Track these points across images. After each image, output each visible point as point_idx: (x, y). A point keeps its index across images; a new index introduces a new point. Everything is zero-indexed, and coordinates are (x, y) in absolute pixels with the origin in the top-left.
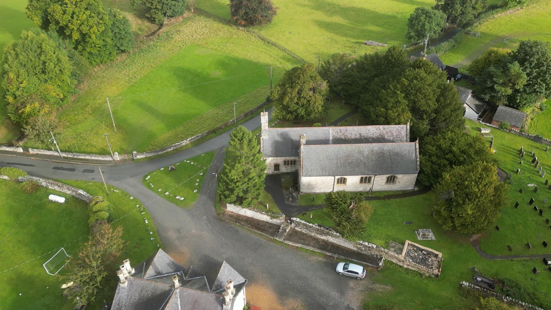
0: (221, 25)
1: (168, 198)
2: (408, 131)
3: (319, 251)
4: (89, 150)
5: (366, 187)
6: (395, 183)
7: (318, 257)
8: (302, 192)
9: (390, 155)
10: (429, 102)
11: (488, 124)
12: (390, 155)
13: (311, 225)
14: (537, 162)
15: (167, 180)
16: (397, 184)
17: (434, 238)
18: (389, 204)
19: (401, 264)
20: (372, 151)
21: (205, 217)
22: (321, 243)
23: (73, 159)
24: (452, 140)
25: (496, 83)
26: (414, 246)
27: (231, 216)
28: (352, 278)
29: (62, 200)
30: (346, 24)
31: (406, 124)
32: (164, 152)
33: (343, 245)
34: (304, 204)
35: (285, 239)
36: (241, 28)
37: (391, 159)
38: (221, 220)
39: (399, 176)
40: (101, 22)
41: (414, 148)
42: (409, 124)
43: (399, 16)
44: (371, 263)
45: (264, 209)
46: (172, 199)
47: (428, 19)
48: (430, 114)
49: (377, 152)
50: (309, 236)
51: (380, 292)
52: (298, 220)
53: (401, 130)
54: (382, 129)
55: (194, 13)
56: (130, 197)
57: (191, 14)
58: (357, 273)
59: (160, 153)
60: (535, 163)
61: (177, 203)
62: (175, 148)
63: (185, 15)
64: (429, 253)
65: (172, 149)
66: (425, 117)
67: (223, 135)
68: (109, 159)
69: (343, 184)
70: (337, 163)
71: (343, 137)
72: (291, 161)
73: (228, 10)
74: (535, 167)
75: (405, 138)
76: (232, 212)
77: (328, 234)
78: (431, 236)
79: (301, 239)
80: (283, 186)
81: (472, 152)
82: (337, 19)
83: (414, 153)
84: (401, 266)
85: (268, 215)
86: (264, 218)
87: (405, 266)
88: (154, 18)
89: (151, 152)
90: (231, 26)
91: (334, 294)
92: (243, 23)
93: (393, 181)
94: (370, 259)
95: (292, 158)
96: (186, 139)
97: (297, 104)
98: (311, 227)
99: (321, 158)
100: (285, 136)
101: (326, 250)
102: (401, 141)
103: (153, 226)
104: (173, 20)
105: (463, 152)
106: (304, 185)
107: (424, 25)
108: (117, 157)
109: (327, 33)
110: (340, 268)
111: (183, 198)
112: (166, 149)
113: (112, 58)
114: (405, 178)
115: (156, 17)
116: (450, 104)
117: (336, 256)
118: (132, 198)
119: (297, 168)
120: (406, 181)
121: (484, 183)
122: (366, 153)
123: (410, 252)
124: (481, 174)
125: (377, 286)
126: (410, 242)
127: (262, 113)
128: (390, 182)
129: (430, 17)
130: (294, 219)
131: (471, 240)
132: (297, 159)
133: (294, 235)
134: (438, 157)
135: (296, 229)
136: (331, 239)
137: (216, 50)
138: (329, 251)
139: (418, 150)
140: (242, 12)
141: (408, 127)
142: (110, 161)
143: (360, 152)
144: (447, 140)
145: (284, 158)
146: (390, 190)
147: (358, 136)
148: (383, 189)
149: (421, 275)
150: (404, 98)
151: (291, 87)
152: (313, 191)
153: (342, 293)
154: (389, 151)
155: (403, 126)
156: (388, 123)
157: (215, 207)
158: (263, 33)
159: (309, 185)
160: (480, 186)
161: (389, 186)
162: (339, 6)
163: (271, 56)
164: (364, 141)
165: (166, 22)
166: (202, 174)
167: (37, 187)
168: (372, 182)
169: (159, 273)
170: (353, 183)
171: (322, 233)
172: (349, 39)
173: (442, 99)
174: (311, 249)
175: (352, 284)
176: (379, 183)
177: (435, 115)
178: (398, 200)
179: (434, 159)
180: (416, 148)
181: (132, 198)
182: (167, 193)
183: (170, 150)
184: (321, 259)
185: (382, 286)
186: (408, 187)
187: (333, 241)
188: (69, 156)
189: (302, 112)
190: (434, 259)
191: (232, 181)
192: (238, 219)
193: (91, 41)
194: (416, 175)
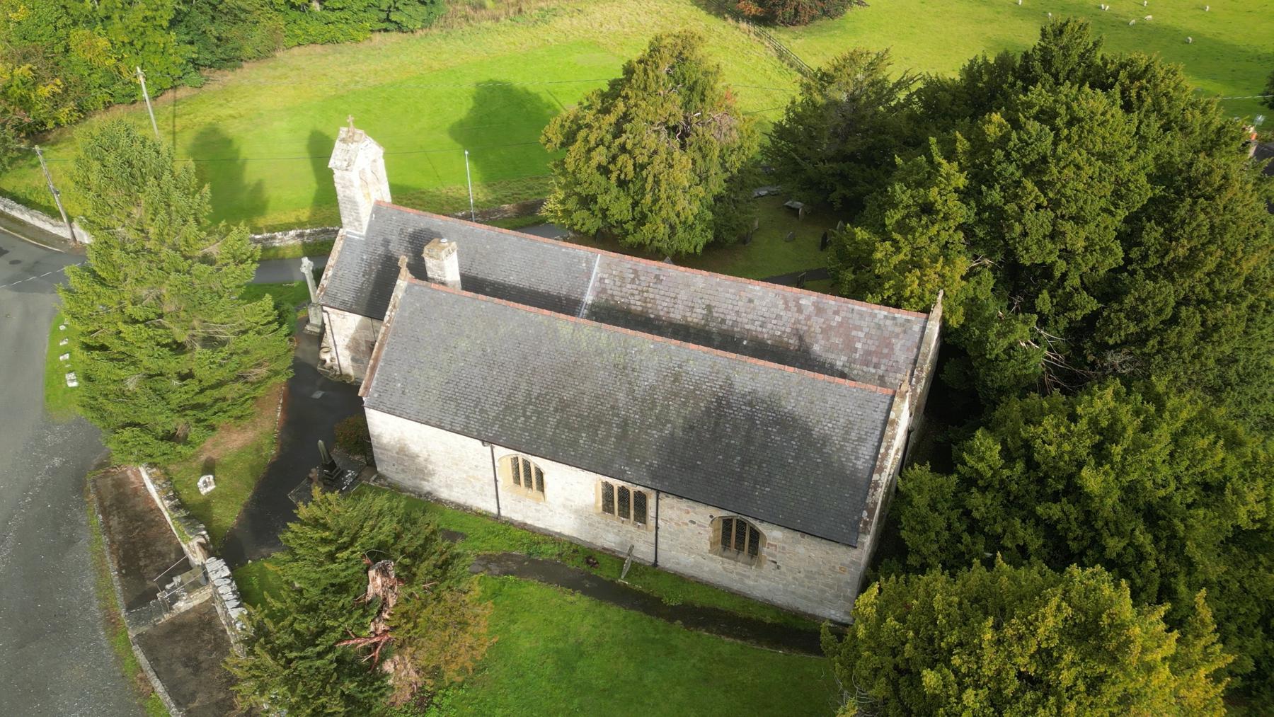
5: (612, 534)
6: (759, 566)
8: (380, 477)
9: (750, 418)
10: (1068, 226)
12: (750, 418)
16: (767, 567)
20: (677, 378)
24: (1107, 435)
27: (120, 484)
37: (749, 440)
39: (773, 535)
41: (879, 417)
42: (937, 312)
48: (1070, 295)
49: (697, 386)
66: (1044, 302)
69: (534, 491)
70: (516, 388)
71: (637, 305)
81: (1201, 528)
83: (873, 440)
90: (725, 19)
93: (754, 551)
99: (464, 345)
105: (1153, 516)
106: (384, 448)
116: (1188, 264)
122: (649, 378)
124: (1047, 657)
128: (740, 547)
134: (1012, 503)
141: (934, 328)
142: (66, 240)
144: (1083, 424)
146: (736, 586)
147: (696, 317)
148: (705, 575)
152: (427, 487)
156: (858, 292)
159: (403, 455)
161: (729, 564)
164: (718, 340)
168: (651, 523)
170: (567, 501)
173: (1153, 234)
176: (682, 535)
178: (727, 645)
179: (979, 503)
189: (620, 208)
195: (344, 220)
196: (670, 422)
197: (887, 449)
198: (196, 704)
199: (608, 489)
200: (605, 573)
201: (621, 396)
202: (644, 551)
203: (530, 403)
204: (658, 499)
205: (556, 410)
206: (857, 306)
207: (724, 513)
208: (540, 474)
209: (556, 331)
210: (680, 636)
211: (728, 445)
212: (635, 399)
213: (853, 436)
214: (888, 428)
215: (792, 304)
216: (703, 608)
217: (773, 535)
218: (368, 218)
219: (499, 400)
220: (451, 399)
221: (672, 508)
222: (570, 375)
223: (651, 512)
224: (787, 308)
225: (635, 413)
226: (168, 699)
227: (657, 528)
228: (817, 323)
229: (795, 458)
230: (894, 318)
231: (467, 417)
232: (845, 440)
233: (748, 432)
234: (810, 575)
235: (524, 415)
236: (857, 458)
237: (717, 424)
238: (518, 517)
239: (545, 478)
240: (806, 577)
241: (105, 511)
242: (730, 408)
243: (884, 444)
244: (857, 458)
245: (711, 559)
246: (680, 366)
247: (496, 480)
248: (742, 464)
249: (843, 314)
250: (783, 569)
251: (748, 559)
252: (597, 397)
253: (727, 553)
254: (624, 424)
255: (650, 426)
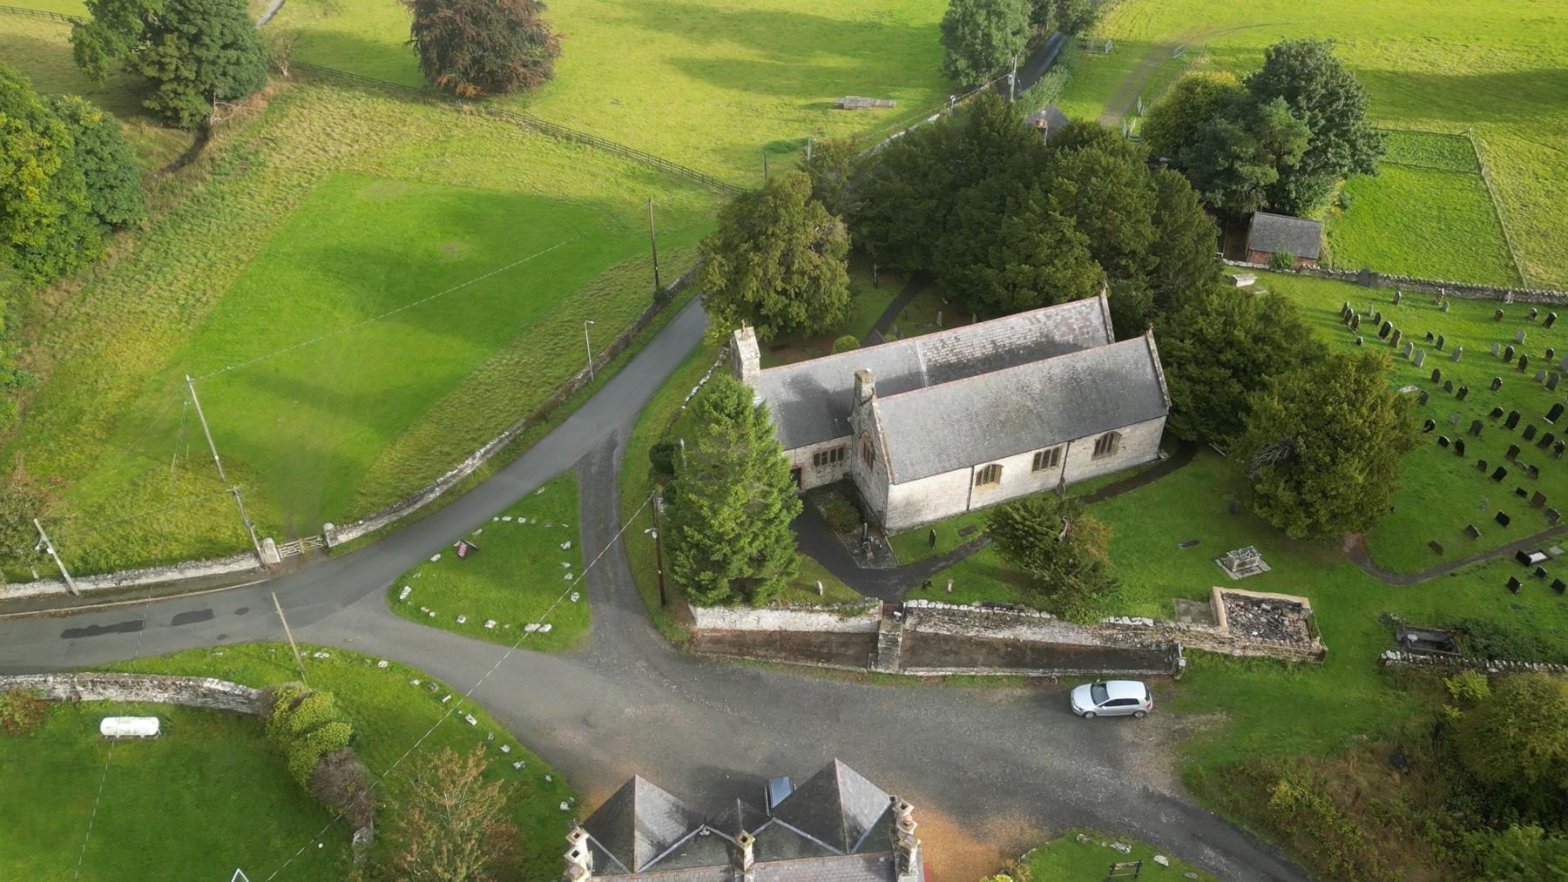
0: (398, 107)
1: (500, 636)
2: (1107, 313)
3: (1007, 672)
4: (156, 552)
5: (1051, 477)
7: (1009, 690)
11: (1244, 264)
13: (964, 608)
14: (1397, 333)
15: (469, 584)
16: (1120, 451)
17: (1266, 567)
19: (1226, 650)
20: (1050, 379)
21: (641, 664)
22: (1003, 650)
23: (119, 591)
25: (1238, 157)
26: (1237, 597)
28: (1120, 718)
29: (148, 726)
30: (756, 59)
31: (1098, 294)
32: (418, 505)
33: (1061, 640)
34: (912, 559)
35: (903, 666)
36: (466, 107)
37: (1099, 392)
38: (693, 660)
41: (1145, 351)
42: (1104, 294)
43: (886, 22)
44: (1150, 667)
45: (812, 598)
46: (511, 635)
47: (994, 19)
50: (962, 641)
51: (1206, 733)
52: (924, 604)
53: (1085, 314)
54: (1043, 319)
55: (295, 78)
56: (375, 662)
57: (286, 85)
58: (1135, 702)
59: (405, 513)
60: (1390, 335)
61: (537, 643)
62: (445, 487)
63: (269, 90)
64: (1276, 606)
65: (438, 492)
67: (571, 420)
68: (248, 563)
69: (991, 485)
71: (953, 359)
72: (833, 452)
73: (414, 60)
74: (1393, 344)
75: (1102, 332)
76: (714, 630)
77: (1018, 621)
78: (1258, 563)
79: (945, 653)
80: (840, 523)
82: (724, 49)
84: (1226, 656)
85: (832, 612)
86: (822, 621)
87: (1238, 653)
88: (176, 111)
89: (379, 516)
91: (1098, 772)
92: (471, 90)
94: (1141, 658)
95: (835, 443)
96: (471, 453)
97: (784, 292)
98: (965, 614)
100: (803, 386)
101: (1025, 666)
102: (1095, 342)
103: (499, 728)
104: (236, 108)
105: (1257, 339)
107: (987, 38)
108: (273, 553)
109: (719, 91)
110: (1083, 699)
111: (548, 627)
112: (422, 496)
113: (91, 253)
115: (181, 105)
117: (1056, 673)
118: (383, 664)
119: (847, 469)
120: (1140, 441)
121: (1370, 400)
122: (1037, 387)
123: (1234, 613)
125: (1190, 721)
126: (1224, 591)
127: (738, 333)
129: (1000, 15)
130: (913, 604)
131: (1347, 550)
132: (849, 443)
133: (921, 649)
134: (1200, 363)
135: (921, 629)
136: (1025, 634)
137: (420, 179)
138: (1036, 666)
139: (1156, 355)
140: (464, 59)
141: (1105, 301)
143: (1023, 389)
145: (814, 447)
147: (989, 350)
149: (1283, 664)
150: (1076, 228)
151: (757, 248)
152: (918, 519)
153: (1115, 762)
154: (1091, 371)
156: (1048, 302)
157: (656, 627)
158: (537, 111)
159: (910, 506)
160: (1364, 410)
162: (714, 11)
163: (593, 174)
165: (215, 118)
166: (568, 545)
167: (42, 707)
169: (660, 846)
170: (1017, 474)
171: (1002, 623)
172: (787, 99)
174: (985, 671)
175: (1126, 732)
176: (1080, 461)
177: (1158, 260)
178: (1135, 493)
179: (1192, 369)
180: (1150, 352)
181: (383, 664)
182: (491, 624)
183: (432, 496)
184: (1018, 692)
185: (1203, 718)
186: (1143, 455)
187: (1033, 638)
188: (103, 585)
189: (799, 312)
190: (1294, 616)
191: (719, 538)
192: (742, 643)
193: (25, 208)
228: (1051, 324)
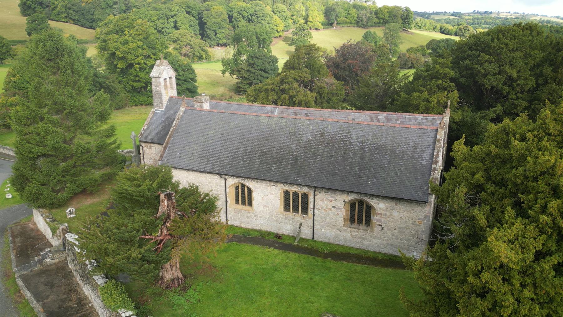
6: (372, 230)
9: (363, 149)
12: (363, 149)
16: (377, 229)
18: (328, 269)
20: (322, 135)
39: (379, 206)
40: (152, 56)
41: (431, 140)
49: (333, 137)
69: (246, 207)
70: (238, 149)
83: (429, 151)
93: (368, 222)
99: (212, 133)
114: (395, 214)
155: (435, 117)
161: (355, 232)
168: (310, 212)
176: (328, 217)
178: (359, 267)
194: (429, 210)
195: (155, 104)
196: (319, 155)
197: (438, 152)
198: (49, 300)
199: (287, 193)
200: (286, 241)
201: (293, 146)
202: (306, 233)
203: (246, 155)
204: (315, 195)
205: (260, 156)
206: (407, 116)
207: (352, 197)
208: (250, 191)
209: (259, 121)
210: (330, 263)
211: (351, 162)
212: (301, 147)
213: (418, 150)
214: (437, 143)
215: (374, 119)
216: (342, 253)
217: (379, 206)
218: (166, 103)
219: (230, 155)
220: (205, 157)
221: (322, 200)
222: (267, 140)
223: (311, 205)
224: (372, 120)
225: (301, 153)
226: (33, 298)
227: (314, 215)
229: (389, 164)
230: (427, 119)
231: (213, 165)
232: (414, 152)
233: (362, 155)
234: (401, 231)
235: (243, 160)
236: (422, 160)
237: (345, 153)
238: (236, 224)
239: (254, 194)
240: (400, 232)
241: (14, 236)
242: (351, 145)
243: (436, 151)
244: (422, 160)
245: (344, 231)
246: (324, 129)
247: (226, 201)
248: (360, 169)
249: (400, 120)
250: (386, 229)
251: (365, 228)
252: (281, 148)
253: (353, 226)
254: (296, 159)
255: (309, 158)
